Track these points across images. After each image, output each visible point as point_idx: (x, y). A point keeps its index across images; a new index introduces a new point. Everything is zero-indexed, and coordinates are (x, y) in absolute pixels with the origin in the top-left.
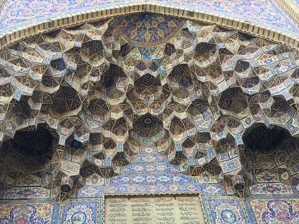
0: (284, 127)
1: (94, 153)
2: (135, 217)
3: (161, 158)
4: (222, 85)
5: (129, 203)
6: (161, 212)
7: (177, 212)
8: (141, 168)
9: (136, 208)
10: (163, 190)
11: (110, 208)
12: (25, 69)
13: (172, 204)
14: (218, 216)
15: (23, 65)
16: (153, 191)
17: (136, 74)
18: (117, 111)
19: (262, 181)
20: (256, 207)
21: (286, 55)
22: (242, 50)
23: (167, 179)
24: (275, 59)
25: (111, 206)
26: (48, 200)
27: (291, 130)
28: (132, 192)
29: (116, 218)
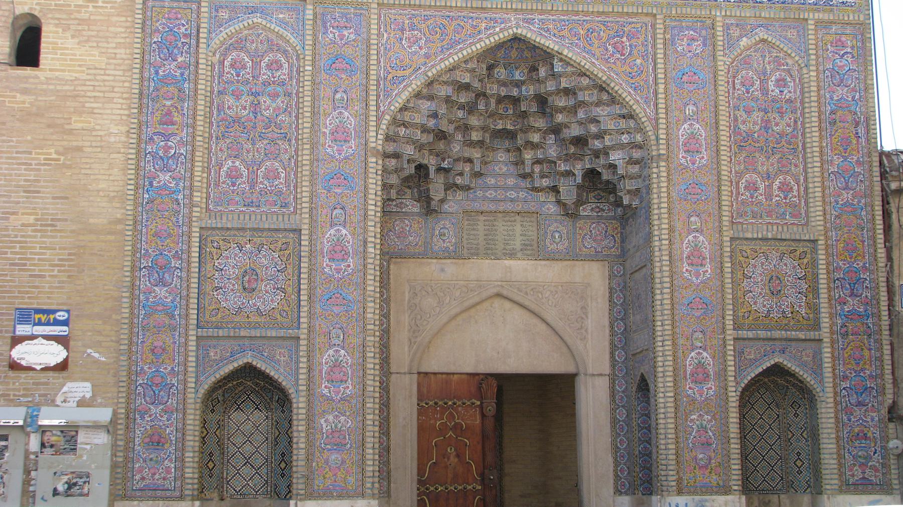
0: (614, 181)
1: (456, 173)
2: (486, 232)
3: (512, 168)
4: (575, 131)
5: (482, 218)
6: (506, 228)
7: (518, 229)
8: (493, 181)
9: (487, 223)
10: (509, 206)
11: (467, 223)
12: (408, 132)
13: (515, 221)
14: (549, 237)
15: (406, 127)
16: (501, 209)
17: (499, 95)
18: (477, 130)
19: (593, 200)
20: (580, 228)
21: (632, 123)
22: (599, 104)
23: (512, 194)
24: (623, 124)
25: (468, 220)
26: (419, 214)
27: (618, 187)
28: (485, 208)
29: (472, 232)
